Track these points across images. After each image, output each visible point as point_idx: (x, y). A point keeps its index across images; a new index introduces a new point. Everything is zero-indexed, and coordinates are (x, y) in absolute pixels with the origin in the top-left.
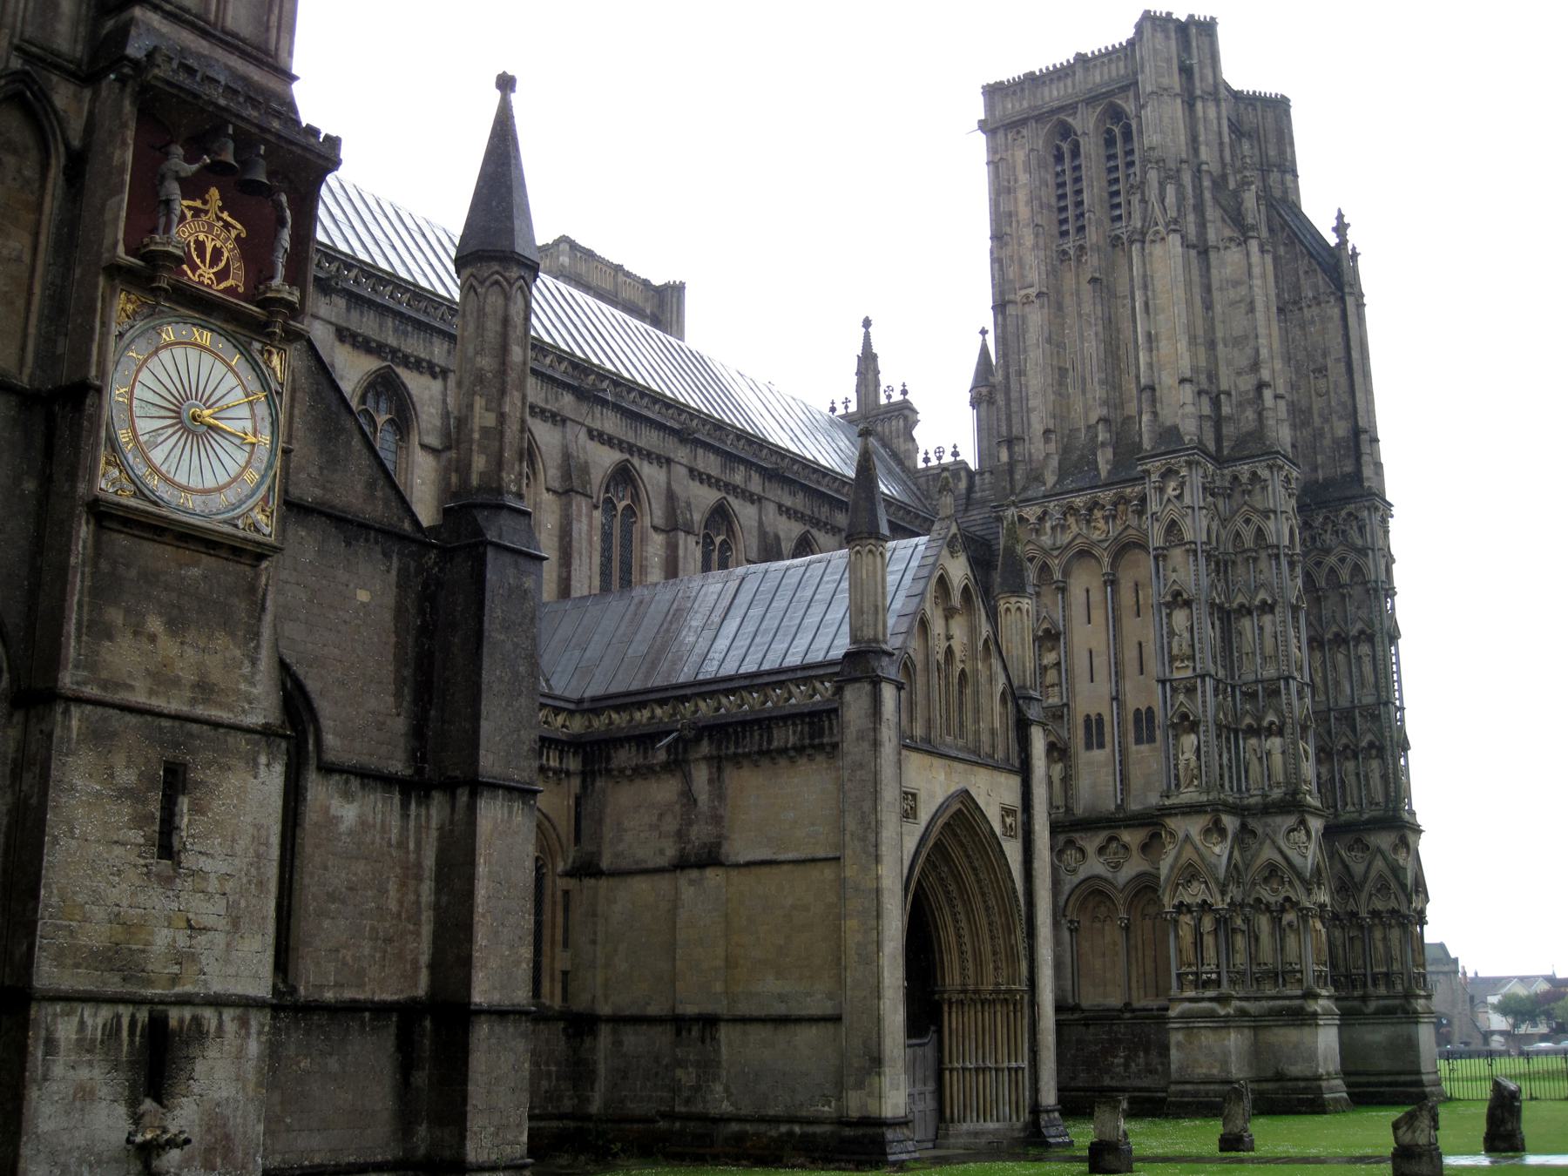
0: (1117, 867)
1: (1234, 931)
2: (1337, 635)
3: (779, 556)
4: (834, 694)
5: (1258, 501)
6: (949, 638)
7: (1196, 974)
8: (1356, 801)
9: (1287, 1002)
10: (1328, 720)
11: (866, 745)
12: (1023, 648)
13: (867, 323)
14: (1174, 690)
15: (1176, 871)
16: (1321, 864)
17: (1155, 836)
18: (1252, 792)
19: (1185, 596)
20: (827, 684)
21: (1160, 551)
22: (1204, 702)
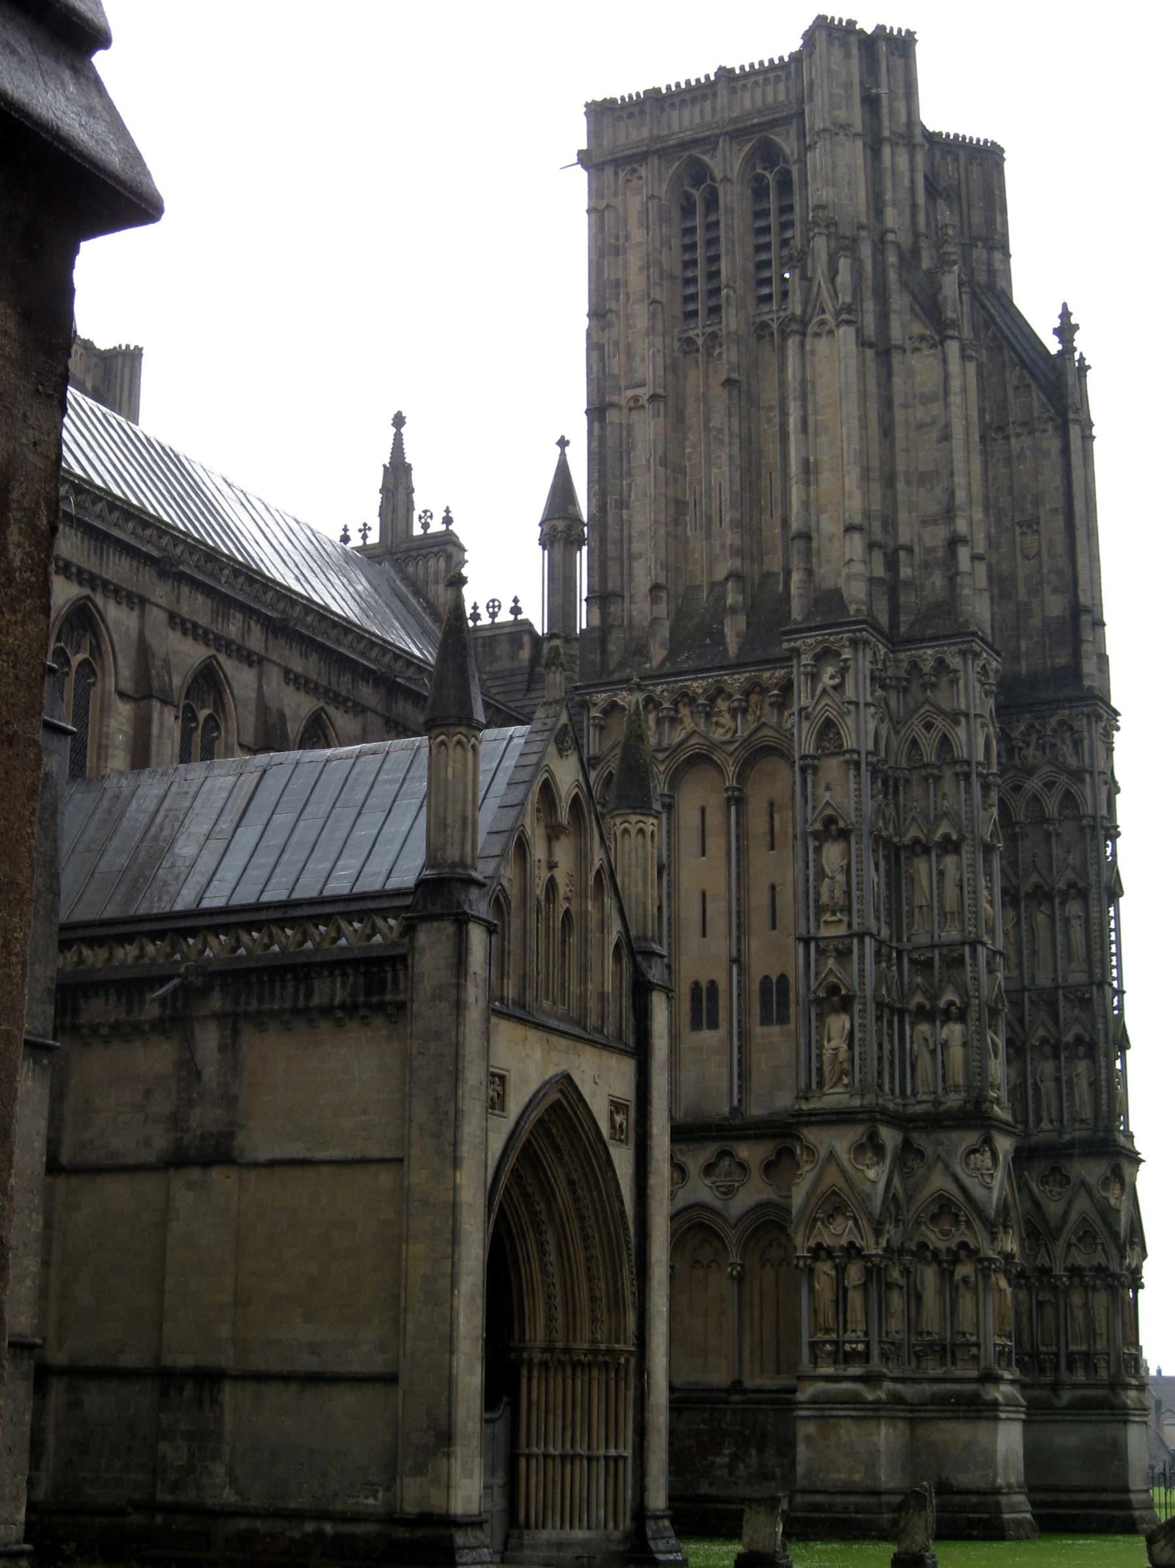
0: (729, 1192)
1: (890, 1286)
2: (1038, 887)
3: (282, 744)
4: (403, 935)
5: (943, 699)
6: (552, 866)
8: (1054, 1116)
9: (957, 1387)
11: (444, 1007)
12: (645, 884)
13: (399, 421)
14: (821, 952)
15: (813, 1200)
16: (1010, 1198)
17: (785, 1153)
18: (920, 1097)
19: (841, 824)
20: (392, 922)
21: (809, 761)
22: (862, 971)
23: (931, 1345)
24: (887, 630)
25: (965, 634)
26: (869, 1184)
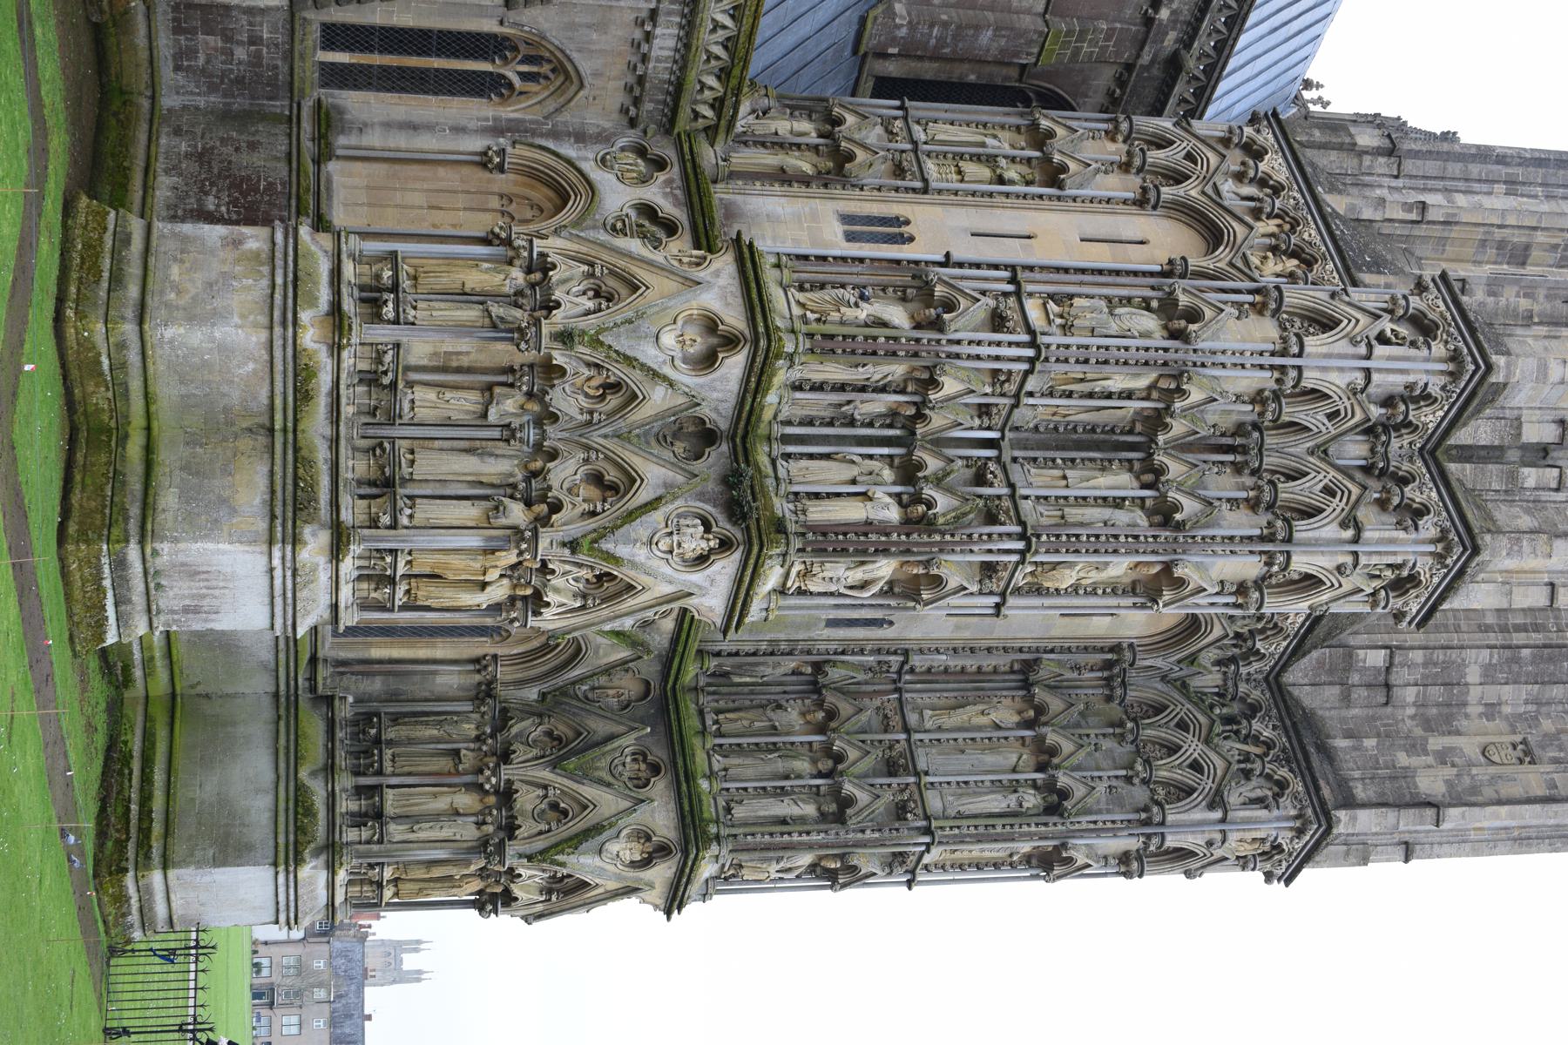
2: (1053, 751)
7: (395, 288)
15: (621, 263)
16: (631, 603)
18: (780, 462)
19: (1192, 327)
23: (396, 464)
24: (1452, 441)
25: (1472, 537)
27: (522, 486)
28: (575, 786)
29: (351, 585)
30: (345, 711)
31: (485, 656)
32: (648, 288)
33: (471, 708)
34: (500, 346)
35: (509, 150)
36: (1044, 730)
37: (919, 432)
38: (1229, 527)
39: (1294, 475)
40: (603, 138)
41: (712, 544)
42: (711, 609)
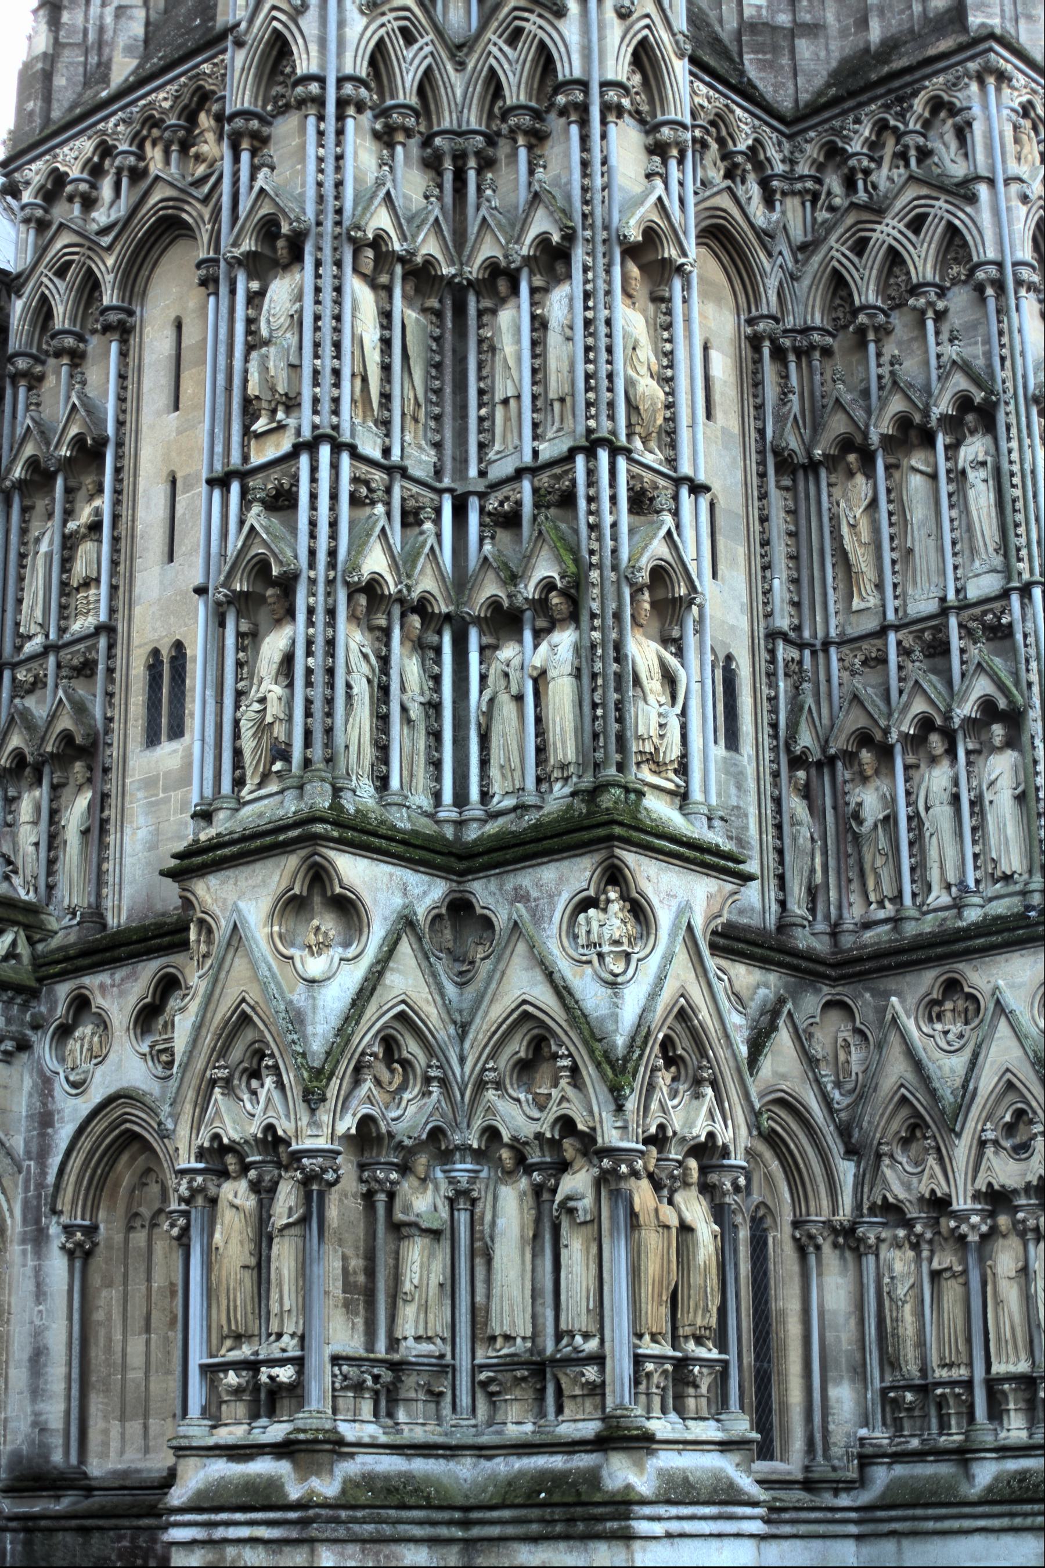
1: (399, 1230)
2: (904, 422)
7: (253, 1366)
9: (557, 1462)
10: (883, 661)
15: (208, 1040)
16: (705, 1014)
19: (285, 229)
21: (239, 123)
23: (511, 1363)
26: (301, 987)
27: (537, 1177)
28: (979, 1100)
29: (690, 1423)
30: (881, 1436)
31: (794, 1238)
32: (243, 1000)
33: (871, 1258)
34: (333, 1212)
35: (65, 1219)
36: (874, 438)
37: (444, 610)
38: (569, 168)
39: (494, 85)
40: (45, 1084)
41: (613, 895)
42: (710, 897)
